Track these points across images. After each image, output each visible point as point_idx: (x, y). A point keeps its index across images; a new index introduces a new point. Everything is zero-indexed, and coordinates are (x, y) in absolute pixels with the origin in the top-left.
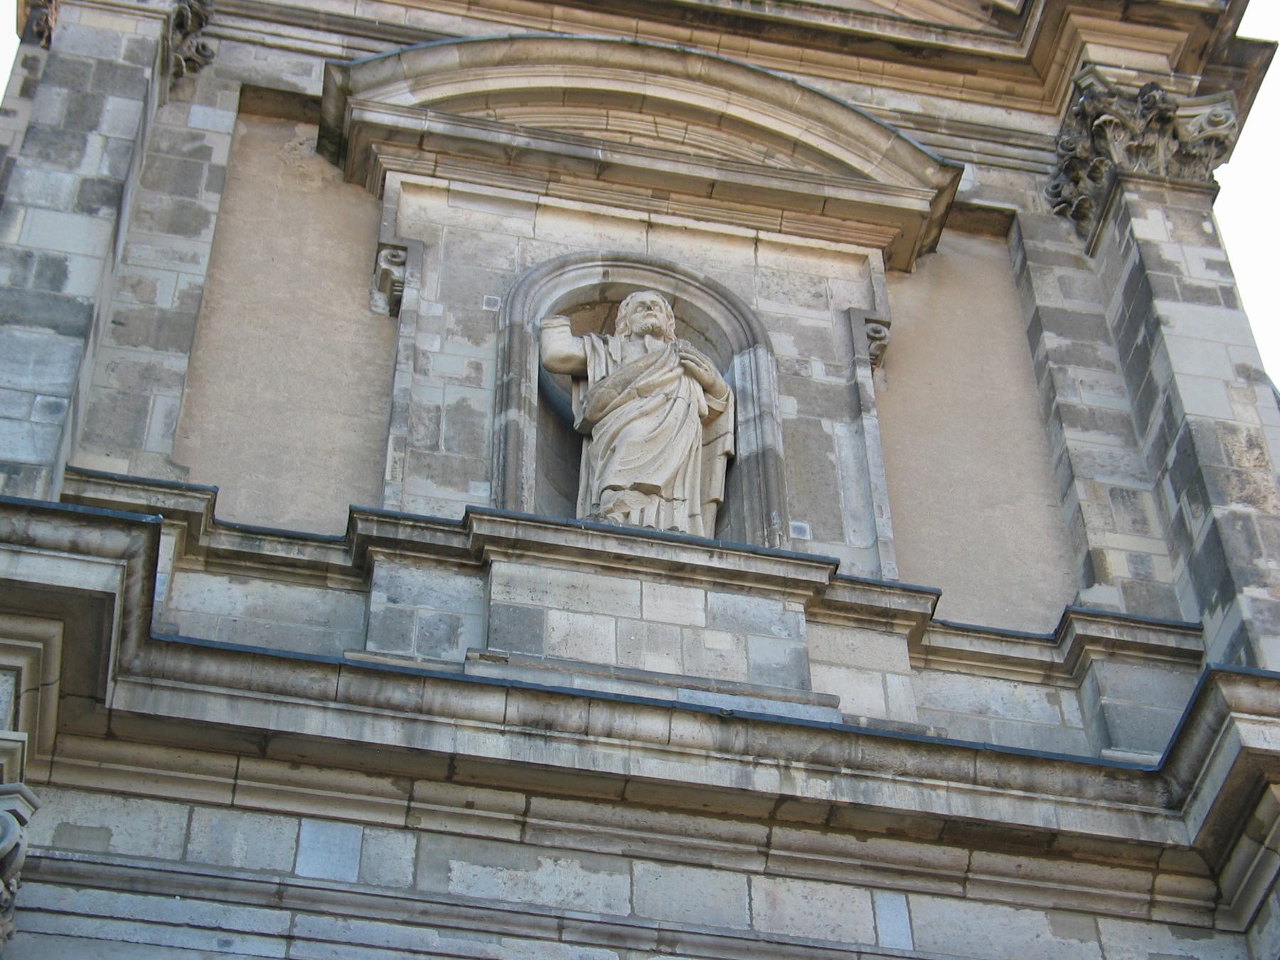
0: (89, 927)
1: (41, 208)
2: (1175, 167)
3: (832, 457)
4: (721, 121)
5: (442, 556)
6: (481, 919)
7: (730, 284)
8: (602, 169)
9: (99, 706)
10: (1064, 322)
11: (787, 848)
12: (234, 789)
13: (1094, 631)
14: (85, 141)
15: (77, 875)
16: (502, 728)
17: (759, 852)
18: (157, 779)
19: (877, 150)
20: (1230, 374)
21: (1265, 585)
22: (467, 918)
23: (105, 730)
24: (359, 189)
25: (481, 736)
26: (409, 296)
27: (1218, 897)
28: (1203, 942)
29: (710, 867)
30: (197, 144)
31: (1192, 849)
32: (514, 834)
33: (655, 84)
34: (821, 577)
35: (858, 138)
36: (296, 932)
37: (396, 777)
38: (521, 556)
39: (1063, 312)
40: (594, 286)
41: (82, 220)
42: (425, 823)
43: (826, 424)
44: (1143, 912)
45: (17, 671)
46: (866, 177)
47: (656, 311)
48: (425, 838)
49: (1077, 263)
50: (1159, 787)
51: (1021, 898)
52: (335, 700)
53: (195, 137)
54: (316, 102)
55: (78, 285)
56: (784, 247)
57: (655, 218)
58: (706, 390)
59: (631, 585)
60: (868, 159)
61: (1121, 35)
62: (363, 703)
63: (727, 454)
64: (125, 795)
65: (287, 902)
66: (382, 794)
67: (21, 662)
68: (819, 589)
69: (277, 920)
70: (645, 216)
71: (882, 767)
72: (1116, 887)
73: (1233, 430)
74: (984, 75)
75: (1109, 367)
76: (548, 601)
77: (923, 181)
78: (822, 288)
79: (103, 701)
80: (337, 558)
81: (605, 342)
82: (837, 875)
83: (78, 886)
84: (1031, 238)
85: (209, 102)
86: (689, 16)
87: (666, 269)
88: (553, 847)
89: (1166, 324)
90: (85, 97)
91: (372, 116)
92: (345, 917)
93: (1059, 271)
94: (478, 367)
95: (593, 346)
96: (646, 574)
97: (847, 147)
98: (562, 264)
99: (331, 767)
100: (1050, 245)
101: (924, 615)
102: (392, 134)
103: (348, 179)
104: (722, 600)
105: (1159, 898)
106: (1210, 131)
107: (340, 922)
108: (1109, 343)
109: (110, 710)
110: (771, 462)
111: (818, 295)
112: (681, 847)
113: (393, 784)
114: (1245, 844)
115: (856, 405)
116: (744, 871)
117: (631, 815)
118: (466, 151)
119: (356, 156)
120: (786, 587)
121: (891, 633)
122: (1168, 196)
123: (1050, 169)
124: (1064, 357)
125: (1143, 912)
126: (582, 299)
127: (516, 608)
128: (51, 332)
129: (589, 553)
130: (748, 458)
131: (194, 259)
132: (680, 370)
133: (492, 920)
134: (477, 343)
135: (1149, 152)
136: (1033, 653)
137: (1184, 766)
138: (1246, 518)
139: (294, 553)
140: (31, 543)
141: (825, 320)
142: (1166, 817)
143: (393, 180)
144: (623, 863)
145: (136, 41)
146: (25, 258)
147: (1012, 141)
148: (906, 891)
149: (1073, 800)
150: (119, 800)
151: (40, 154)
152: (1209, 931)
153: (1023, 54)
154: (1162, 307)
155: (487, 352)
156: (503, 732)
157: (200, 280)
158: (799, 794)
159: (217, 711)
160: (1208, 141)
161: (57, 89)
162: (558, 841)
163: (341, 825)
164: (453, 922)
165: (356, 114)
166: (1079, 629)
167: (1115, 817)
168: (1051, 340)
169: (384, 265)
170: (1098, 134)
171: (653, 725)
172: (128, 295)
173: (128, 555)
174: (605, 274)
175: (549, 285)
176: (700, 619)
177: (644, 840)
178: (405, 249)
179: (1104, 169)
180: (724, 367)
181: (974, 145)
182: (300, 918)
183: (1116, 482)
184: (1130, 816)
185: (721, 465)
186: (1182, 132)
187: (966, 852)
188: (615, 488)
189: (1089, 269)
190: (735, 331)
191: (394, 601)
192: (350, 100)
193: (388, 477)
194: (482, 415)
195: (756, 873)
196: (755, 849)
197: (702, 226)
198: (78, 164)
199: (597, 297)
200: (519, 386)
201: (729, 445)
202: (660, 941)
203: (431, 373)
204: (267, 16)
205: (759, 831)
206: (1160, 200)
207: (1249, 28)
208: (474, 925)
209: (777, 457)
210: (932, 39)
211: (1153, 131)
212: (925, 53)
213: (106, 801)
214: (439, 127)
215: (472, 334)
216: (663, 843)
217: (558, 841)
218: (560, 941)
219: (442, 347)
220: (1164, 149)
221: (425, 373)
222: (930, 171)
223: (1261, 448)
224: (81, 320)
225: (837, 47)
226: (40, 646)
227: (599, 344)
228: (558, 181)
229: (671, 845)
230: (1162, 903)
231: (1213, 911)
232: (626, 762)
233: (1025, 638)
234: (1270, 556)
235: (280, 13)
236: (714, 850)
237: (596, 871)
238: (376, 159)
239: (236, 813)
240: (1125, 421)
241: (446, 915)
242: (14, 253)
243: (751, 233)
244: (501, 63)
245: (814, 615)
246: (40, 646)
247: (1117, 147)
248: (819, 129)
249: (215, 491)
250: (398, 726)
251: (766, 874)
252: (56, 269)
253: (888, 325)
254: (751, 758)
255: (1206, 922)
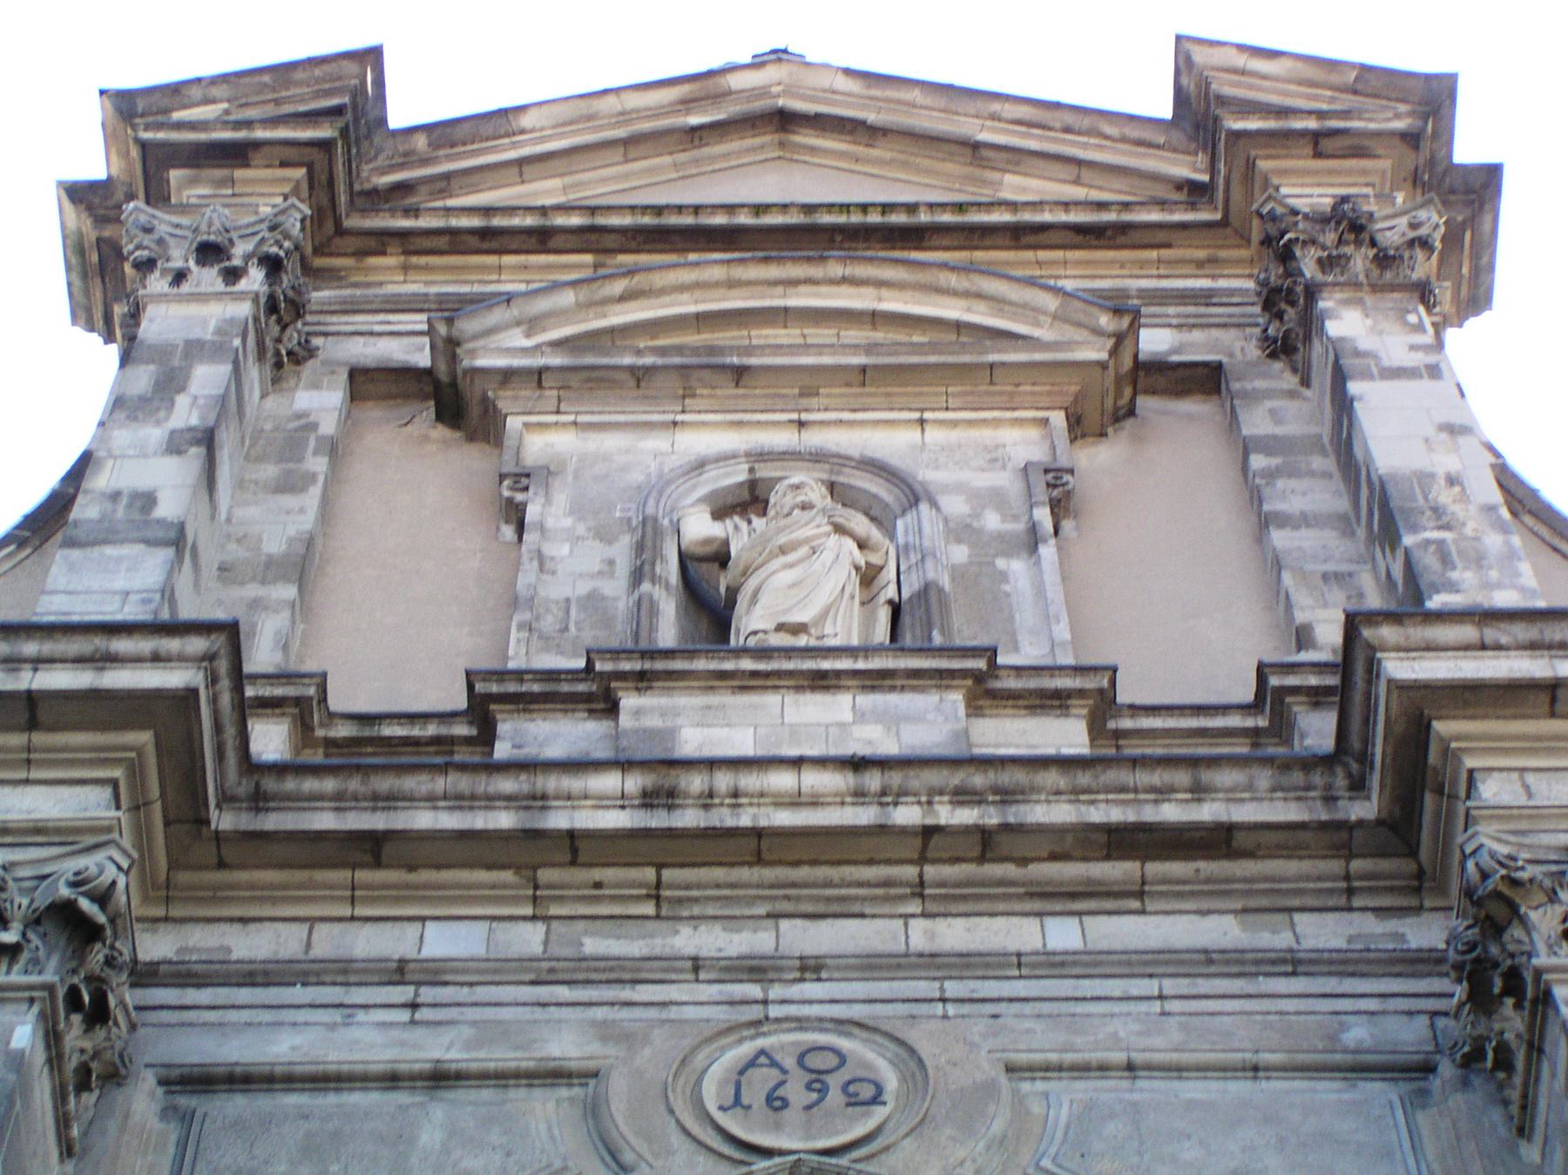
0: (211, 1016)
1: (129, 457)
2: (1376, 273)
3: (1007, 588)
4: (875, 318)
5: (567, 701)
6: (611, 970)
7: (895, 461)
8: (740, 374)
9: (204, 829)
10: (1268, 445)
11: (942, 884)
12: (353, 900)
13: (1292, 681)
14: (172, 402)
15: (196, 975)
16: (619, 803)
17: (914, 895)
18: (274, 901)
19: (1045, 313)
20: (1431, 431)
21: (1457, 591)
22: (596, 970)
23: (215, 860)
24: (484, 446)
25: (600, 813)
26: (532, 513)
27: (1420, 874)
28: (1409, 921)
29: (862, 916)
30: (303, 421)
31: (1379, 822)
32: (649, 909)
33: (797, 295)
34: (981, 664)
35: (1025, 306)
36: (420, 1000)
37: (518, 868)
38: (650, 688)
39: (1275, 438)
40: (741, 484)
41: (172, 462)
42: (554, 910)
43: (1001, 563)
44: (1342, 901)
45: (115, 783)
46: (1037, 339)
47: (807, 489)
48: (555, 924)
49: (1292, 394)
50: (1340, 772)
51: (1205, 904)
52: (445, 798)
53: (299, 416)
54: (428, 372)
55: (168, 508)
56: (954, 424)
57: (804, 416)
58: (862, 546)
59: (772, 700)
60: (1037, 324)
61: (1317, 172)
62: (473, 797)
63: (890, 602)
64: (244, 920)
65: (408, 977)
66: (505, 886)
67: (117, 773)
68: (978, 677)
69: (403, 993)
70: (795, 416)
71: (1034, 789)
72: (1308, 878)
73: (1432, 476)
74: (1180, 246)
75: (1326, 475)
76: (680, 721)
77: (1097, 332)
78: (999, 453)
79: (208, 822)
80: (462, 730)
81: (750, 522)
82: (1001, 907)
83: (198, 986)
84: (1238, 379)
85: (315, 385)
86: (839, 238)
87: (817, 457)
88: (692, 918)
89: (1361, 399)
90: (173, 370)
91: (481, 362)
92: (471, 984)
93: (1269, 404)
94: (611, 563)
95: (736, 528)
96: (788, 687)
97: (1013, 317)
98: (700, 465)
99: (449, 866)
100: (1260, 384)
101: (1101, 691)
102: (507, 376)
103: (471, 438)
104: (867, 700)
105: (1356, 884)
106: (1412, 234)
107: (466, 990)
108: (1325, 455)
109: (217, 832)
110: (933, 596)
111: (995, 460)
112: (829, 899)
113: (516, 873)
114: (1429, 800)
115: (1032, 540)
116: (901, 916)
117: (769, 874)
118: (588, 380)
119: (475, 411)
120: (941, 678)
121: (1067, 715)
122: (1369, 300)
123: (1261, 320)
124: (1271, 475)
125: (1342, 901)
126: (730, 500)
127: (645, 731)
128: (142, 546)
129: (722, 675)
130: (911, 598)
131: (302, 511)
132: (829, 528)
133: (623, 969)
134: (610, 543)
135: (1343, 262)
136: (1235, 721)
137: (1356, 743)
138: (1441, 544)
139: (416, 732)
140: (112, 659)
141: (1004, 479)
142: (1350, 798)
143: (514, 423)
144: (770, 923)
145: (225, 321)
146: (115, 496)
147: (1215, 300)
148: (1080, 914)
149: (1246, 795)
150: (237, 927)
151: (128, 417)
152: (1418, 910)
153: (1218, 216)
154: (1353, 387)
155: (622, 550)
156: (623, 807)
157: (308, 526)
158: (943, 822)
159: (325, 821)
160: (1411, 243)
161: (142, 368)
162: (696, 910)
163: (467, 923)
164: (581, 976)
165: (466, 363)
166: (1274, 681)
167: (1293, 805)
168: (1258, 461)
169: (506, 493)
170: (1286, 256)
171: (783, 780)
172: (232, 546)
173: (210, 657)
174: (751, 470)
175: (688, 484)
176: (848, 716)
177: (788, 898)
178: (528, 476)
179: (1299, 289)
180: (891, 534)
181: (1171, 310)
182: (423, 990)
183: (1330, 567)
184: (1310, 803)
185: (884, 615)
186: (1379, 237)
187: (1137, 864)
188: (755, 633)
189: (1305, 399)
190: (898, 499)
191: (519, 747)
192: (459, 351)
193: (511, 652)
194: (615, 599)
195: (913, 916)
196: (908, 891)
197: (860, 416)
198: (167, 419)
199: (746, 495)
200: (653, 564)
201: (891, 592)
202: (803, 969)
203: (560, 572)
204: (374, 307)
205: (910, 872)
206: (1359, 302)
207: (1468, 149)
208: (603, 977)
209: (941, 591)
210: (1110, 217)
211: (1347, 243)
212: (1109, 233)
213: (225, 927)
214: (556, 360)
215: (603, 535)
216: (811, 898)
217: (696, 910)
218: (697, 980)
219: (571, 552)
220: (1360, 261)
221: (554, 573)
222: (1105, 320)
223: (1461, 484)
224: (172, 534)
225: (1007, 243)
226: (133, 755)
227: (743, 525)
228: (694, 396)
229: (817, 899)
230: (1361, 889)
231: (1418, 890)
232: (755, 817)
233: (1224, 709)
234: (1466, 568)
235: (387, 302)
236: (864, 899)
237: (739, 931)
238: (495, 406)
239: (357, 924)
240: (1343, 518)
241: (575, 970)
242: (103, 494)
243: (916, 415)
244: (622, 298)
245: (981, 708)
246: (133, 755)
247: (1308, 265)
248: (981, 306)
249: (324, 676)
250: (512, 813)
251: (924, 915)
252: (147, 500)
253: (1071, 471)
254: (889, 799)
255: (1414, 902)
